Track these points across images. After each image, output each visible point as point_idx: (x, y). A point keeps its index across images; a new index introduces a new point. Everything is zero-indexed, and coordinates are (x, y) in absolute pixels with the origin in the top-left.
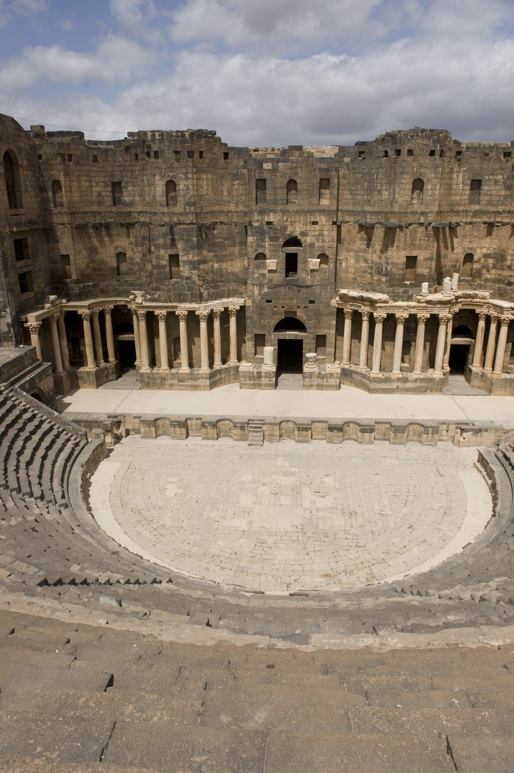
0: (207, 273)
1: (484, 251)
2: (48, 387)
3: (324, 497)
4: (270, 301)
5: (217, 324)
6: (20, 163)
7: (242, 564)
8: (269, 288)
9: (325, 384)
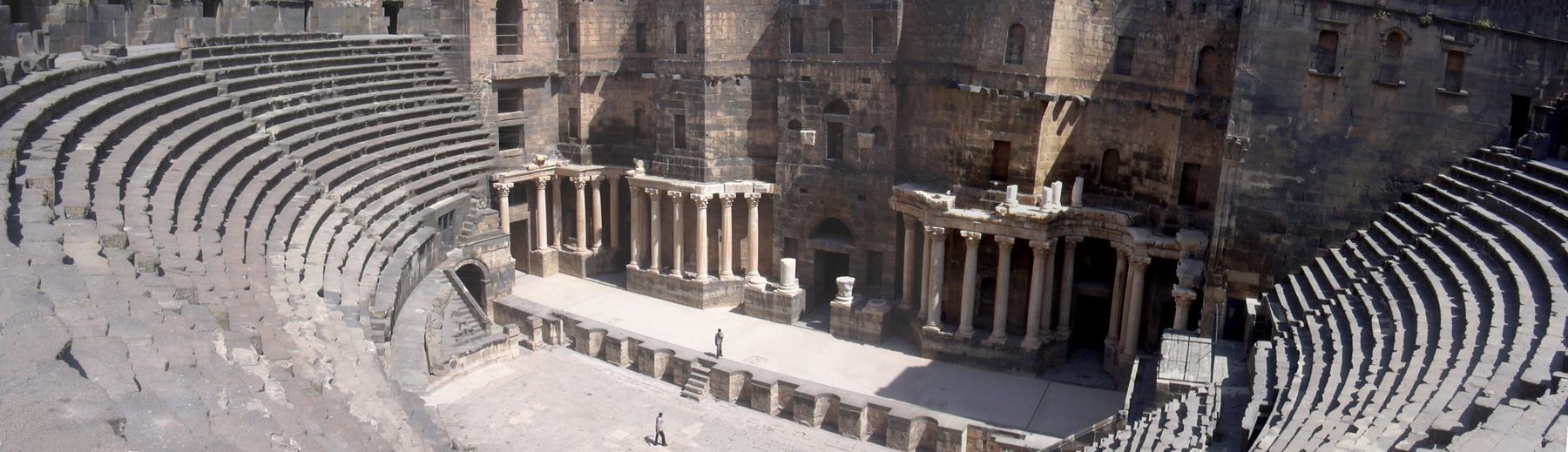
1: (1135, 148)
5: (728, 214)
8: (804, 170)
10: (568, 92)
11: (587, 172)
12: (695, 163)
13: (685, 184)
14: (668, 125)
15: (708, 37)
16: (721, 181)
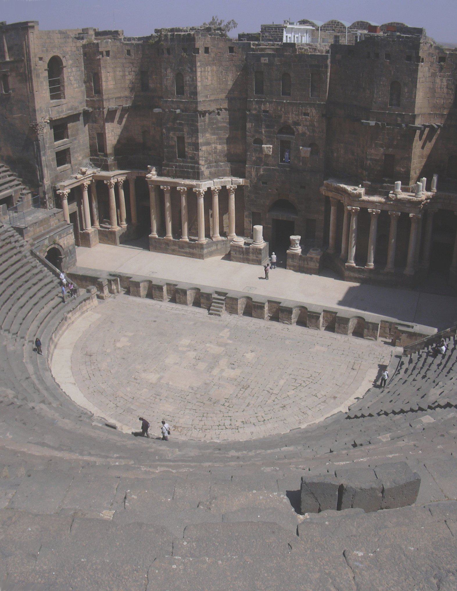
0: (210, 154)
2: (68, 243)
3: (234, 369)
4: (266, 183)
6: (64, 64)
7: (132, 407)
8: (264, 170)
9: (306, 266)
10: (95, 122)
11: (116, 176)
12: (192, 168)
13: (188, 182)
14: (172, 143)
15: (199, 84)
16: (210, 179)
